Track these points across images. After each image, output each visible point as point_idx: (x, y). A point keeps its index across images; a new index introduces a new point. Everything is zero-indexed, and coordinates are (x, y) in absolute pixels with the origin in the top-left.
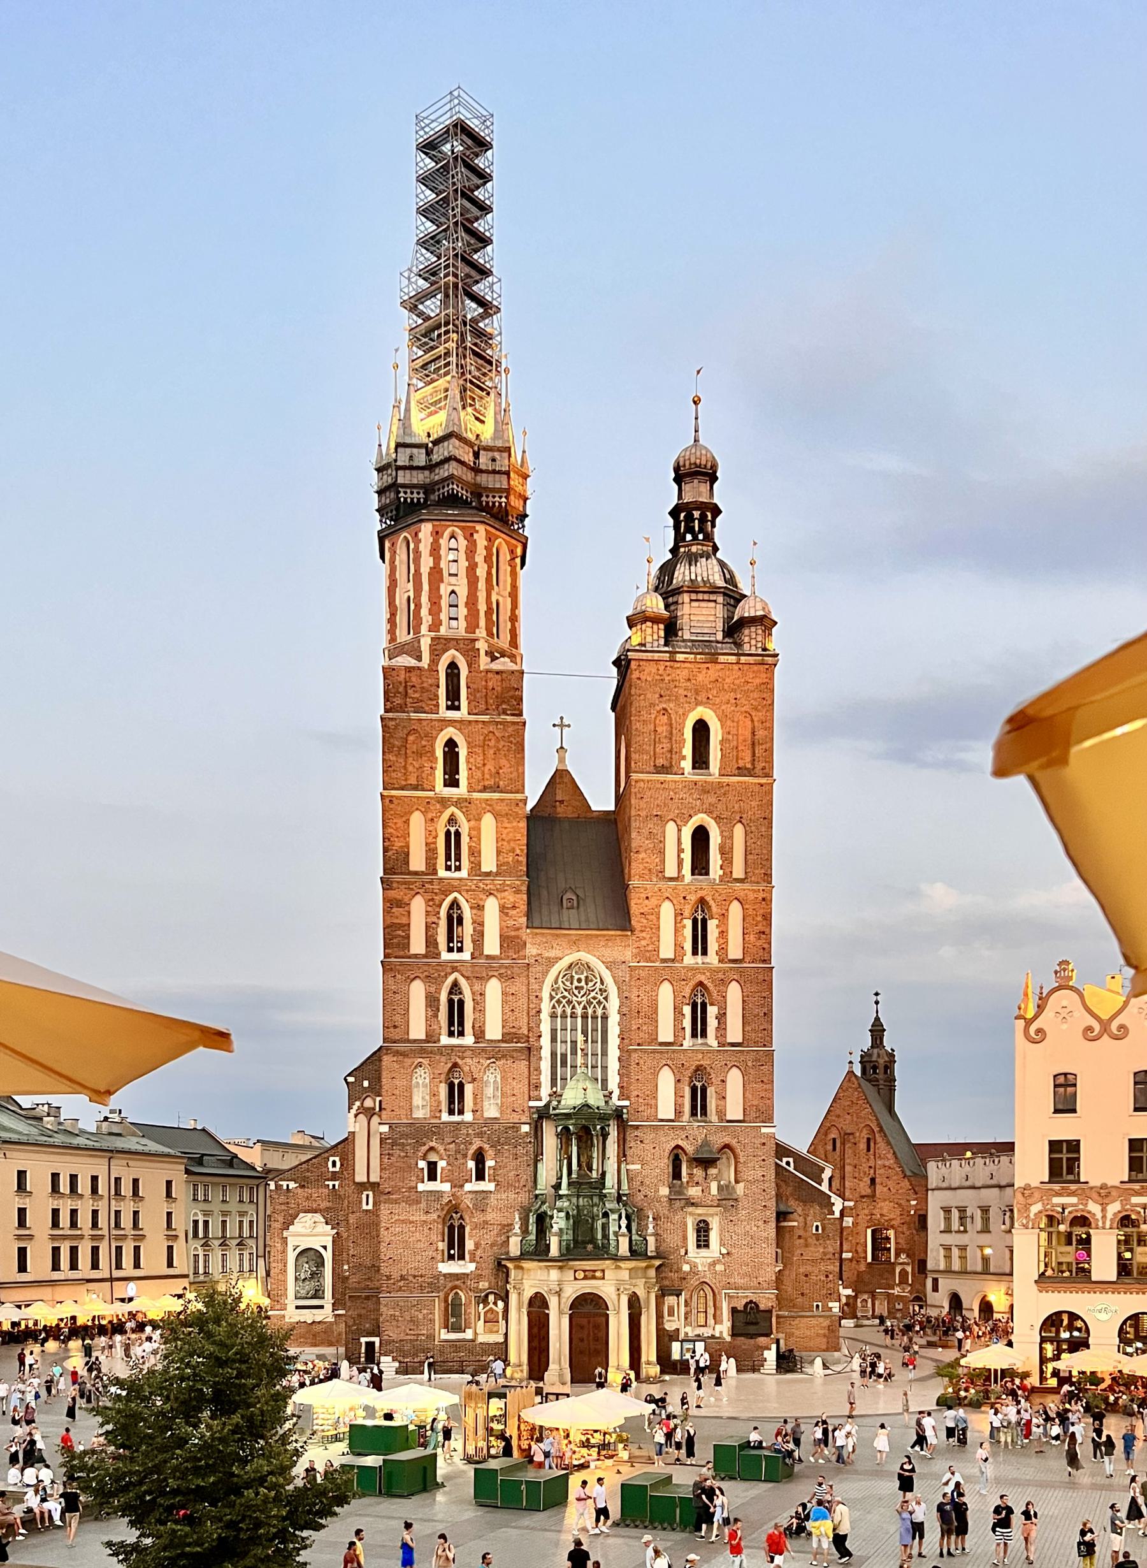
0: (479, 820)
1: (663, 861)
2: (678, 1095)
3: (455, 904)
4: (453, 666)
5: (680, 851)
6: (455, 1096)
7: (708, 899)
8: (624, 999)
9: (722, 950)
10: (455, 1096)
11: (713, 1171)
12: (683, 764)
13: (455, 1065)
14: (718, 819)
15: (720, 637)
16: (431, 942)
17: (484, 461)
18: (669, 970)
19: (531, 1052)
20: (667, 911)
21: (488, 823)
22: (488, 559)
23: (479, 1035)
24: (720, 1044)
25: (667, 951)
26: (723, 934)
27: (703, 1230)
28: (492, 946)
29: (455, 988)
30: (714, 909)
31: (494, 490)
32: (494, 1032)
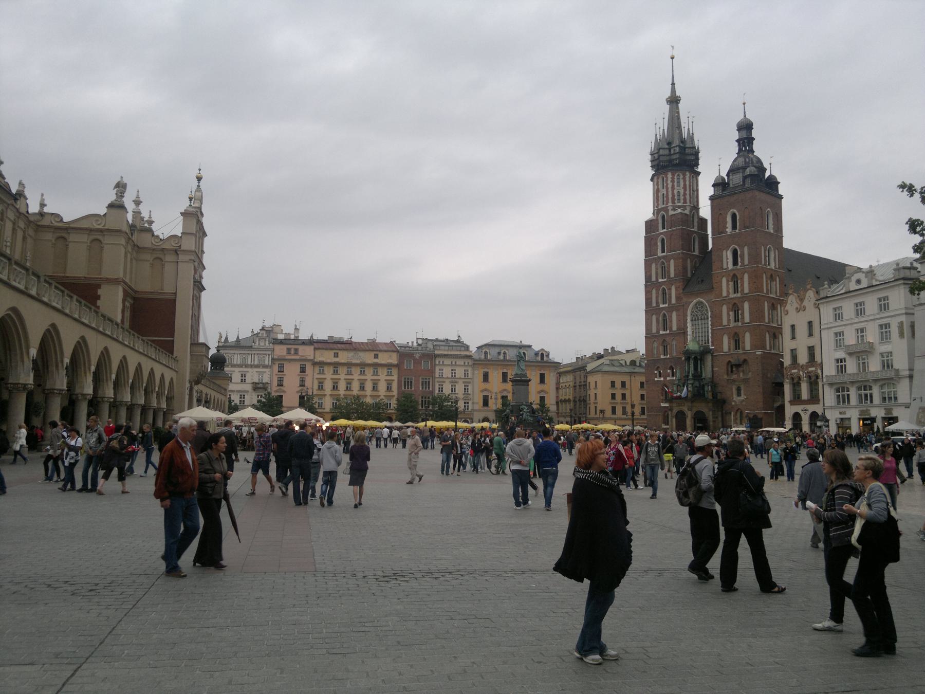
0: (670, 261)
1: (722, 264)
2: (729, 343)
3: (664, 289)
4: (663, 217)
5: (727, 259)
6: (665, 348)
7: (737, 274)
8: (712, 312)
9: (743, 290)
10: (665, 348)
11: (741, 369)
12: (727, 230)
13: (664, 340)
14: (739, 246)
15: (741, 183)
16: (657, 303)
17: (672, 151)
18: (726, 300)
19: (685, 333)
20: (724, 280)
21: (672, 262)
22: (673, 181)
23: (671, 329)
24: (742, 324)
25: (725, 294)
26: (742, 285)
27: (739, 390)
28: (674, 301)
29: (664, 315)
30: (739, 277)
31: (673, 160)
32: (675, 328)
